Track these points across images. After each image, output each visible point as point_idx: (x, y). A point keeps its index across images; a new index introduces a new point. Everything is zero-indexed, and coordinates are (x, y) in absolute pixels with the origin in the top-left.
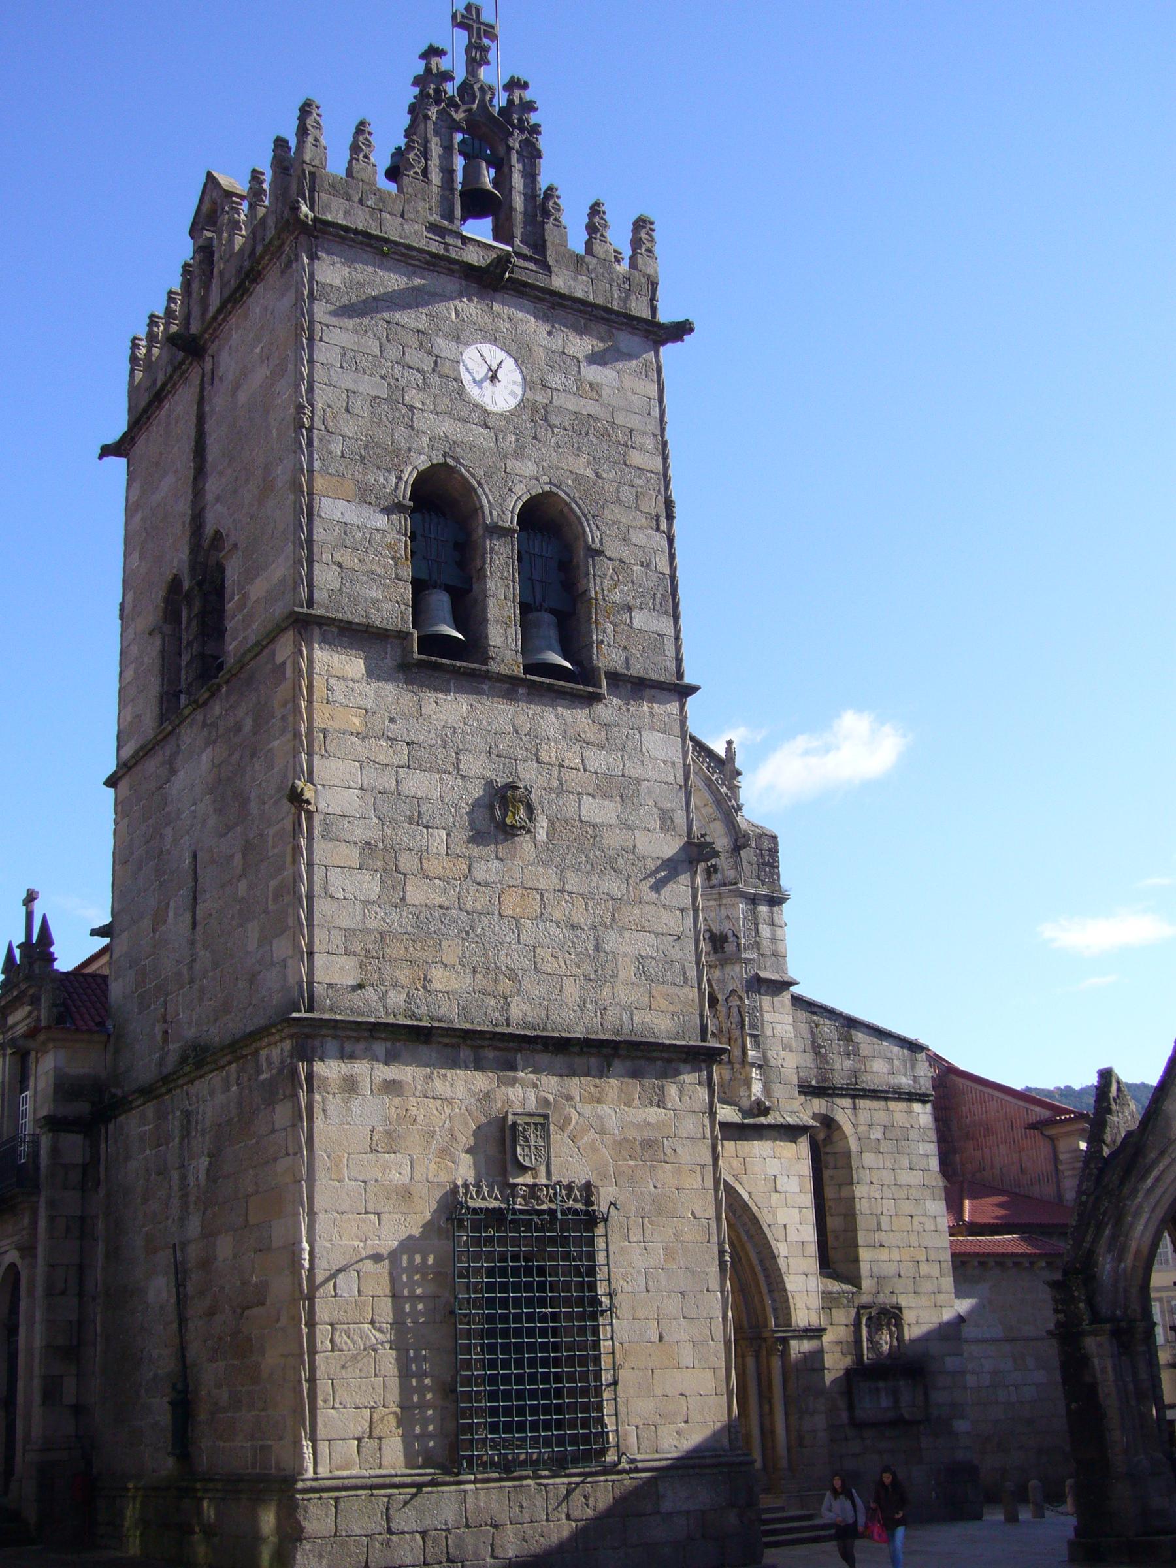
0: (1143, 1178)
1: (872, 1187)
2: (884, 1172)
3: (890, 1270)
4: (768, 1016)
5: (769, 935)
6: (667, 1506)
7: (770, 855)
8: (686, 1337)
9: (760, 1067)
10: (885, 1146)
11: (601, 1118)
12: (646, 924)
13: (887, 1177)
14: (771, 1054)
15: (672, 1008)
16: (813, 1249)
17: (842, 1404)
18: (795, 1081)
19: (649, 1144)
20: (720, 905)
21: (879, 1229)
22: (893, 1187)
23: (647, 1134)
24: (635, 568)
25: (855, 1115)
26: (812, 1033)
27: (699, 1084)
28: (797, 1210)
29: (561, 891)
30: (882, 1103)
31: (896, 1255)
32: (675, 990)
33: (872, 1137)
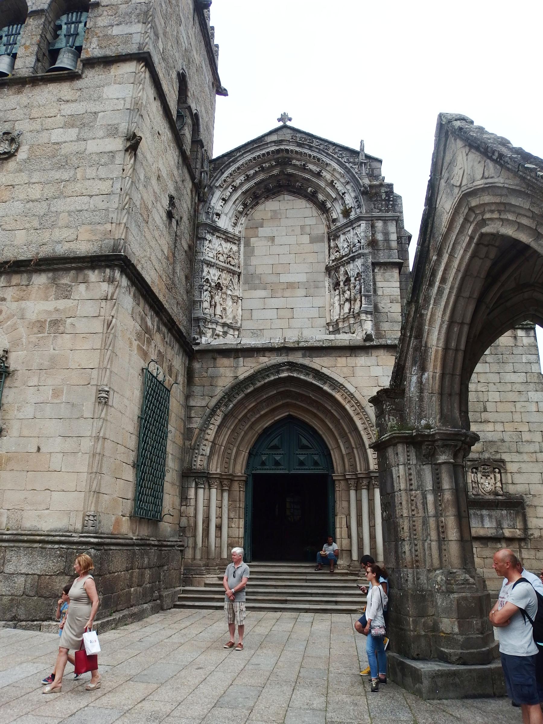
0: (431, 284)
3: (496, 437)
4: (379, 284)
6: (9, 568)
8: (58, 450)
9: (370, 313)
11: (23, 310)
12: (84, 191)
14: (380, 306)
15: (94, 238)
19: (55, 323)
20: (353, 229)
21: (485, 410)
23: (55, 316)
24: (121, 6)
27: (104, 281)
29: (29, 183)
31: (499, 427)
32: (99, 227)
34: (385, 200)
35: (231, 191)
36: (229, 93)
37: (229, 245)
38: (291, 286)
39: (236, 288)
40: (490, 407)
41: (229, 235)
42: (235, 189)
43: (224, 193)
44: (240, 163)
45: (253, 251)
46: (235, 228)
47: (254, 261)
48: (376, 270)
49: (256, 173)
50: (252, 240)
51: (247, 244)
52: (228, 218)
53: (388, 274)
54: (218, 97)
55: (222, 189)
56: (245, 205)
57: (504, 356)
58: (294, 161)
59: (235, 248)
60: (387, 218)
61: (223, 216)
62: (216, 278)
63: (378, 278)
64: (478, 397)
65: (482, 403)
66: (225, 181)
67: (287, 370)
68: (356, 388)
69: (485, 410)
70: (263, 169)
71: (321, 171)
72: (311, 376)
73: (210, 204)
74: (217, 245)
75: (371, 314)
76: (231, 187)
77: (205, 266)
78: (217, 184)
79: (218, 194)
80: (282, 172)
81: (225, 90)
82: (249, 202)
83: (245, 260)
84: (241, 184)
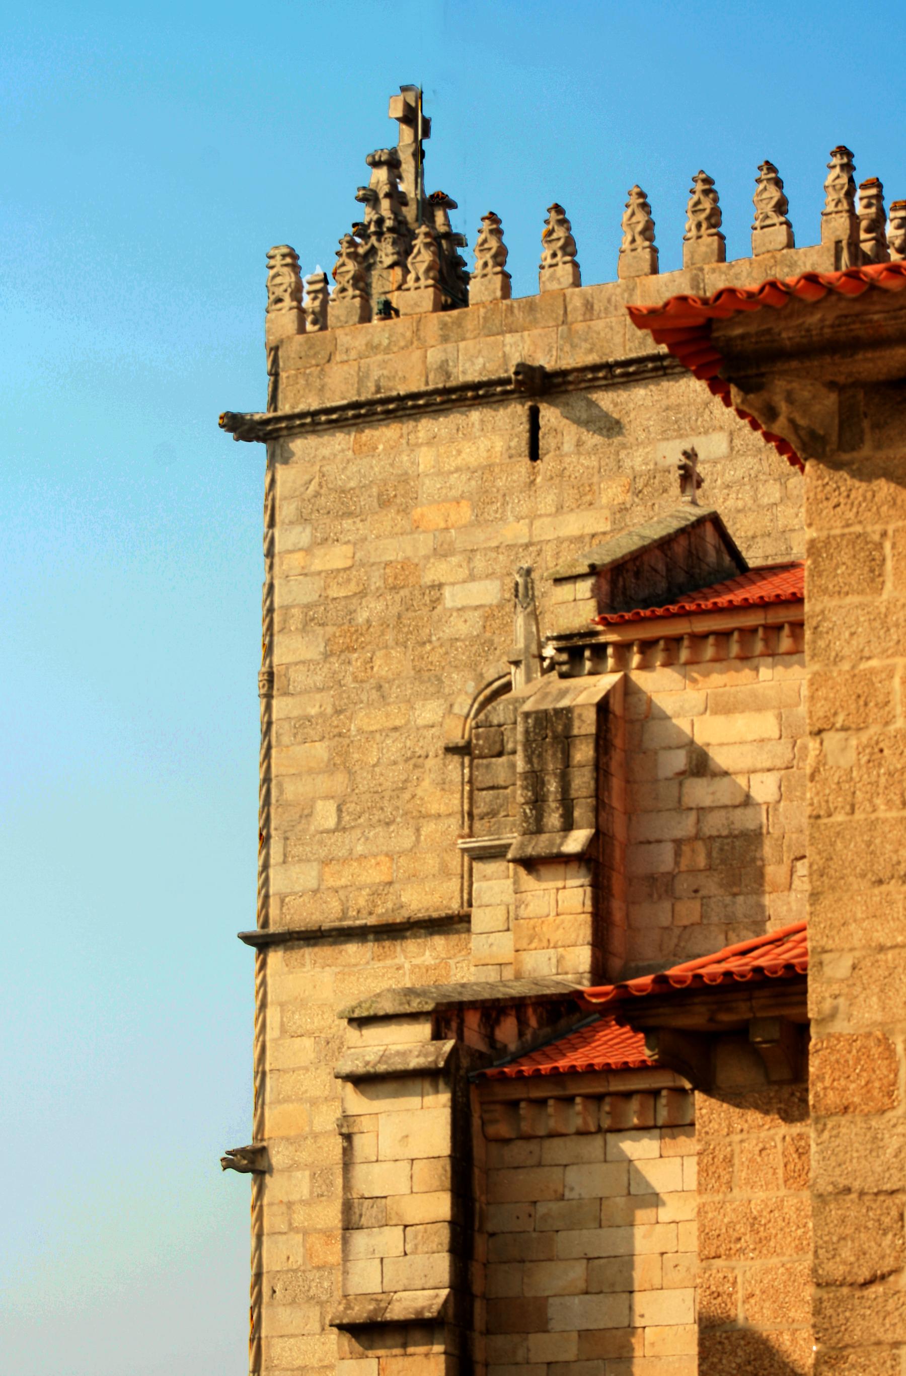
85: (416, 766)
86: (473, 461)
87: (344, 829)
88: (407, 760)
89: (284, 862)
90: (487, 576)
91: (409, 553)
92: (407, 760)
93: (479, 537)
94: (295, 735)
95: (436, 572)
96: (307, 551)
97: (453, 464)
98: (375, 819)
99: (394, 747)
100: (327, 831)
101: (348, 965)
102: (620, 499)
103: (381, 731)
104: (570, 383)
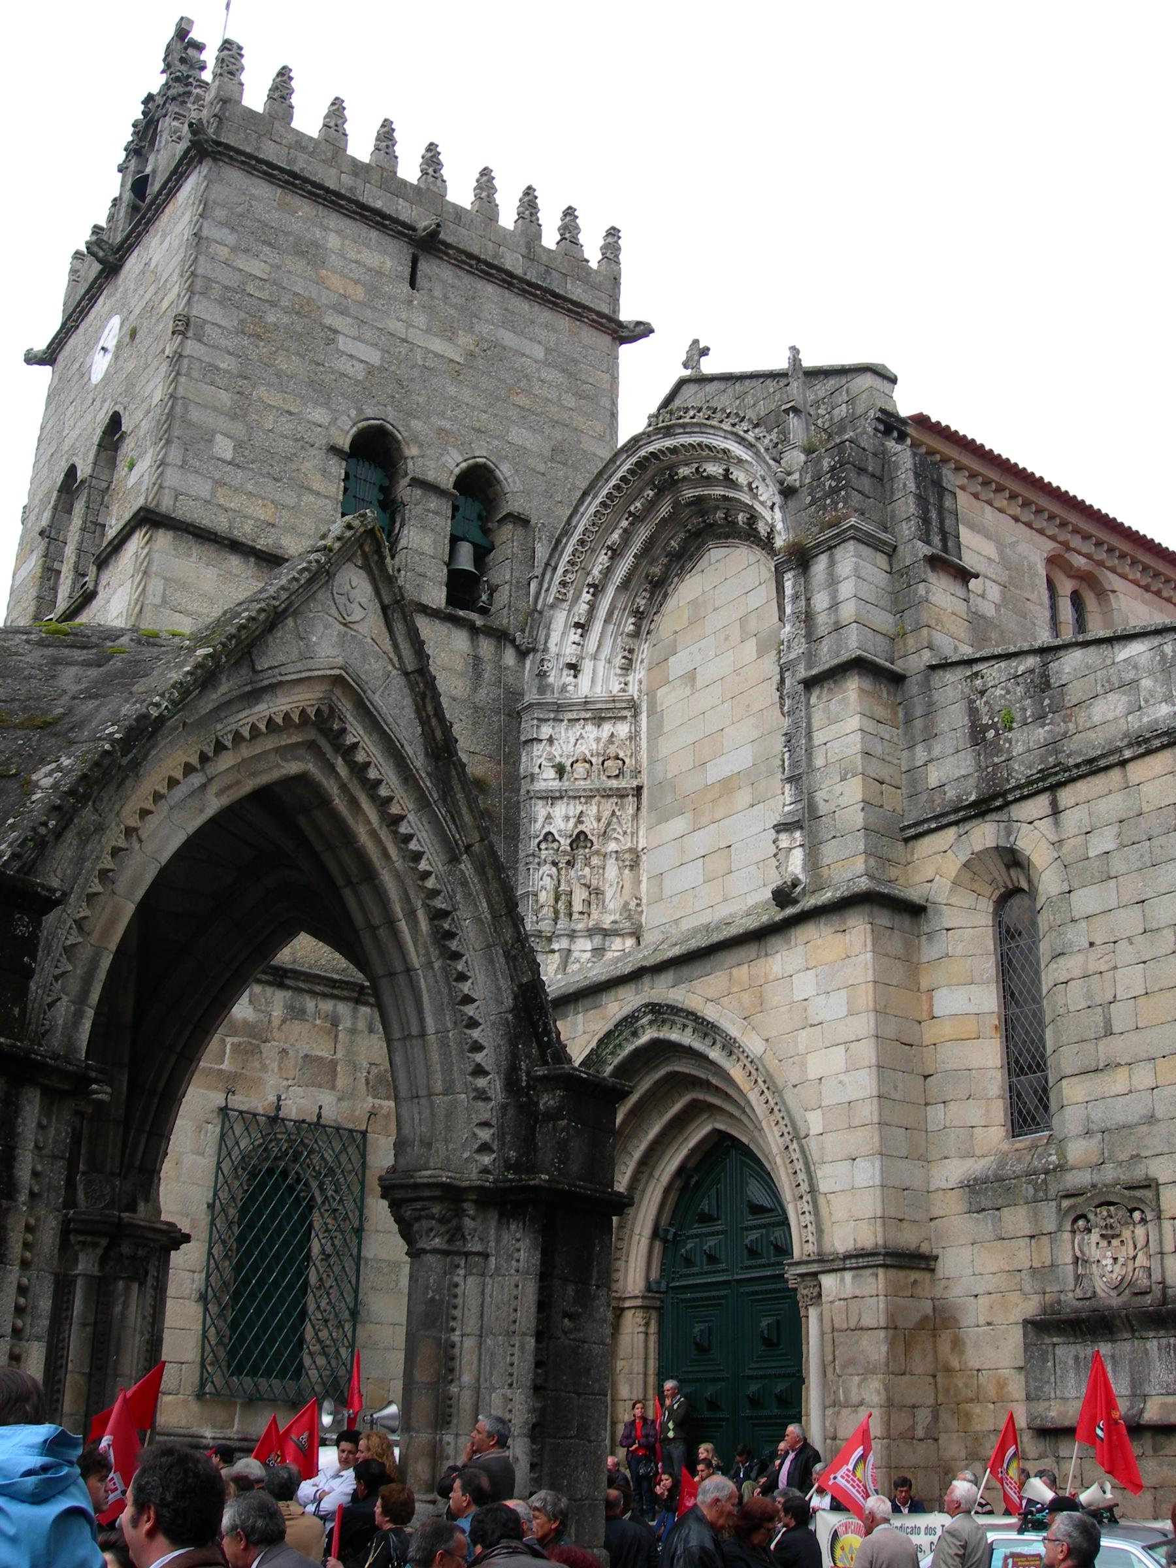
1: (1093, 954)
2: (1122, 914)
4: (819, 737)
5: (826, 605)
7: (832, 478)
10: (1118, 865)
13: (1129, 921)
14: (819, 796)
16: (868, 1111)
17: (1016, 1387)
18: (859, 819)
21: (1109, 1032)
22: (1140, 939)
25: (1057, 824)
26: (973, 712)
28: (842, 1048)
30: (1115, 775)
31: (1143, 1077)
33: (1090, 855)
34: (835, 491)
35: (588, 597)
36: (654, 326)
37: (607, 728)
38: (727, 786)
39: (629, 831)
40: (1121, 1015)
41: (598, 706)
42: (597, 589)
43: (575, 609)
44: (580, 529)
45: (660, 725)
46: (630, 678)
47: (665, 747)
48: (813, 700)
49: (627, 534)
50: (660, 693)
51: (652, 712)
52: (601, 664)
53: (834, 706)
54: (624, 350)
55: (566, 605)
56: (639, 615)
57: (1155, 842)
58: (681, 471)
59: (623, 729)
60: (833, 543)
61: (587, 666)
62: (572, 821)
63: (818, 719)
64: (1089, 995)
65: (1099, 1009)
66: (563, 584)
67: (651, 1023)
68: (767, 1040)
69: (1109, 1032)
70: (636, 519)
71: (727, 470)
72: (689, 1030)
73: (546, 650)
74: (572, 741)
75: (801, 828)
76: (586, 590)
77: (540, 803)
78: (551, 600)
79: (560, 619)
80: (676, 504)
81: (639, 323)
82: (644, 602)
83: (649, 750)
84: (608, 572)
85: (302, 448)
86: (368, 262)
87: (238, 466)
88: (297, 440)
89: (182, 467)
90: (372, 345)
91: (314, 296)
92: (297, 440)
93: (369, 315)
94: (204, 375)
95: (332, 319)
96: (234, 249)
97: (352, 255)
98: (265, 471)
99: (287, 426)
100: (224, 461)
101: (230, 573)
102: (472, 348)
103: (278, 409)
104: (447, 254)
